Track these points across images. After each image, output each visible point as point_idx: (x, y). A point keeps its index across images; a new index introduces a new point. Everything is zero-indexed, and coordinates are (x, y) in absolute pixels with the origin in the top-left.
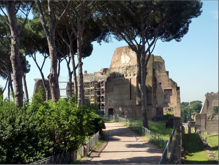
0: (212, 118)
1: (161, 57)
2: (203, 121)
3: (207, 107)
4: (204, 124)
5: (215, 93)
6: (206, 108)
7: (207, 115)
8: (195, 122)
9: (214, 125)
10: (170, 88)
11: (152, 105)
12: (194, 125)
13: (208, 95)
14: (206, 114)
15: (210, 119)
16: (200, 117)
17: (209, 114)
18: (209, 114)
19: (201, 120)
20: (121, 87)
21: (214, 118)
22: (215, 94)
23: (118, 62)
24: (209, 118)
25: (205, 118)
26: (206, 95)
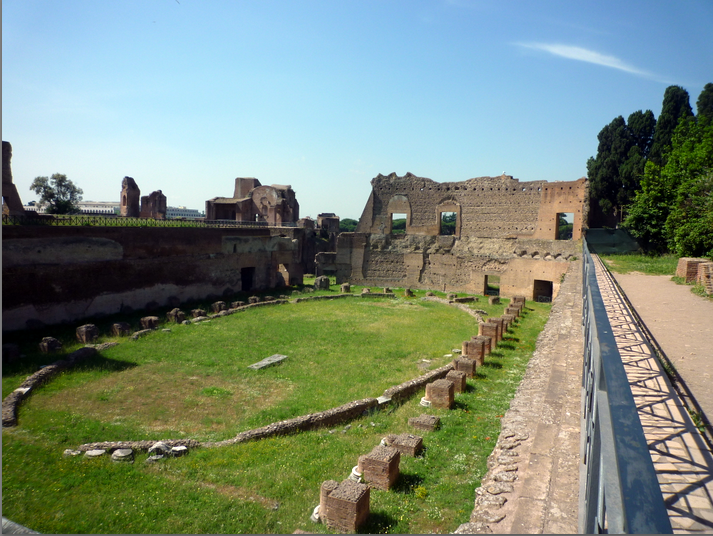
0: (384, 247)
2: (358, 255)
3: (374, 215)
4: (360, 262)
5: (399, 175)
6: (370, 216)
7: (372, 236)
9: (389, 266)
12: (333, 263)
14: (370, 234)
15: (379, 250)
16: (351, 243)
17: (377, 235)
18: (377, 235)
19: (354, 250)
21: (390, 247)
22: (399, 178)
24: (376, 247)
25: (366, 246)
26: (372, 182)
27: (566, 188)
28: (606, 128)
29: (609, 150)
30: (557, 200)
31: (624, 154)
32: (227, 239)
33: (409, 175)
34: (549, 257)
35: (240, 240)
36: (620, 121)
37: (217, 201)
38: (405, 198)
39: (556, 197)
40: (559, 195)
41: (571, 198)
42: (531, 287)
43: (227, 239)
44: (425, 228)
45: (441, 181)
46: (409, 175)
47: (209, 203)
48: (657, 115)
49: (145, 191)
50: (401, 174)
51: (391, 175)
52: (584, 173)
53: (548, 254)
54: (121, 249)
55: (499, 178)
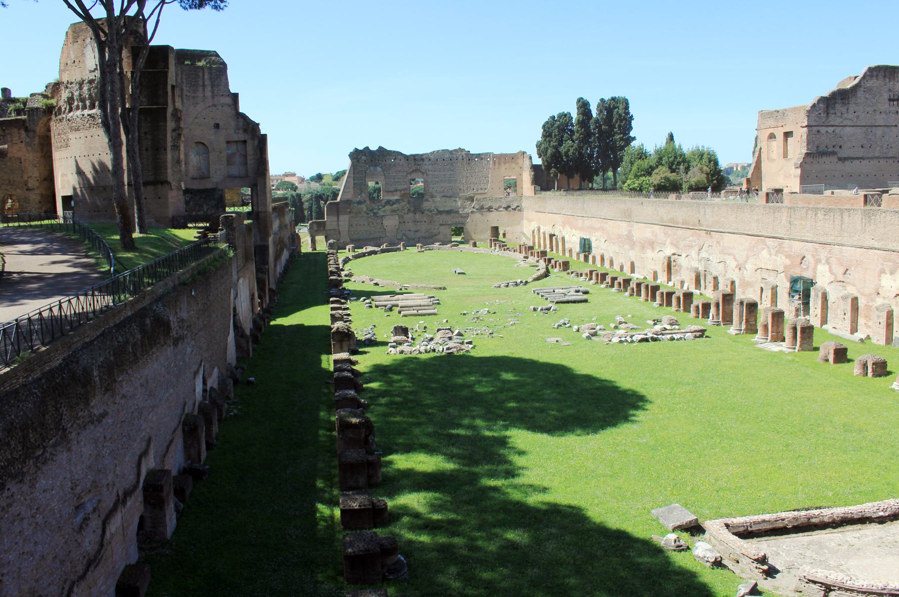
1: (217, 55)
8: (324, 223)
10: (241, 136)
11: (168, 183)
12: (324, 229)
20: (89, 137)
23: (75, 64)
27: (512, 158)
28: (547, 123)
29: (550, 136)
30: (503, 167)
31: (561, 142)
33: (381, 149)
34: (501, 209)
36: (553, 117)
38: (379, 169)
39: (502, 165)
40: (505, 163)
41: (514, 165)
44: (398, 192)
46: (380, 148)
48: (575, 115)
50: (374, 148)
51: (367, 148)
52: (533, 152)
53: (500, 207)
55: (455, 150)
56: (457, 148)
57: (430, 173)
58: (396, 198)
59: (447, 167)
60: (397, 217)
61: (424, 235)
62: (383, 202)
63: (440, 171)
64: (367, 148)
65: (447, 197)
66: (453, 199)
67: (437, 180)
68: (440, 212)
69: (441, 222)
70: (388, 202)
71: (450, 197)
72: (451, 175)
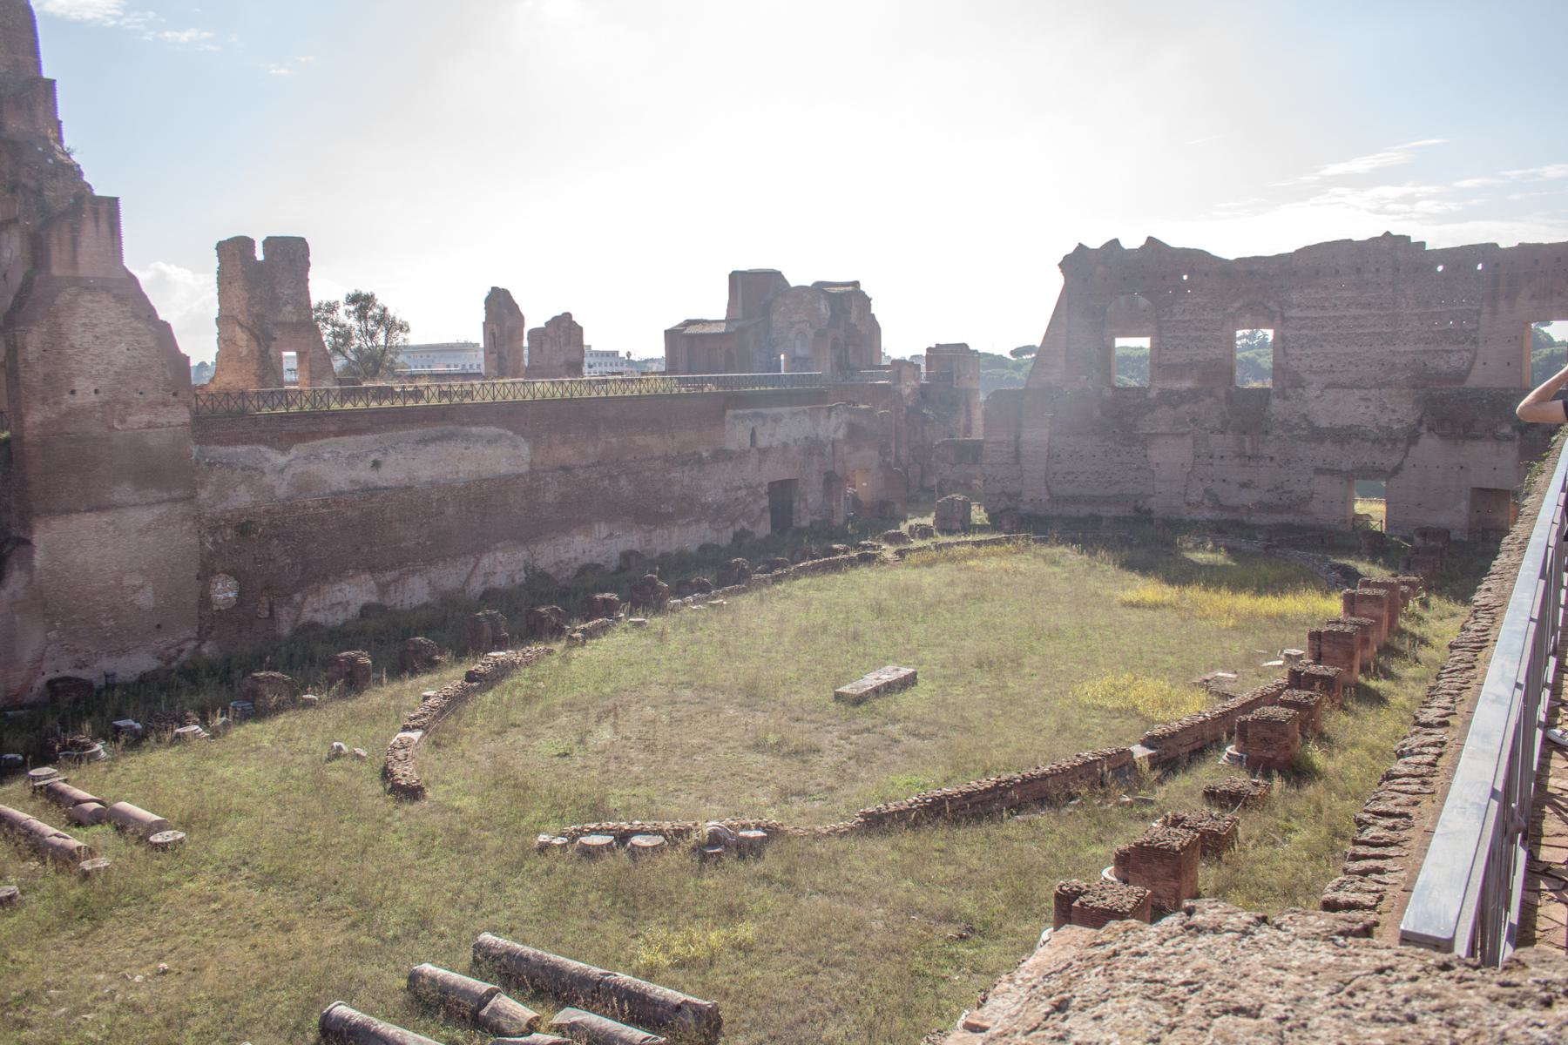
13: (1078, 264)
32: (736, 417)
33: (1150, 240)
35: (763, 416)
37: (691, 330)
42: (1464, 505)
43: (736, 417)
45: (1231, 256)
46: (1150, 240)
47: (671, 335)
49: (535, 317)
50: (1132, 241)
51: (1115, 242)
54: (525, 450)
56: (1380, 234)
57: (1294, 313)
58: (1188, 384)
59: (1345, 294)
60: (1189, 441)
61: (1267, 498)
62: (1153, 394)
63: (1323, 308)
64: (1115, 242)
65: (1343, 386)
66: (1358, 393)
67: (1313, 333)
68: (1318, 435)
69: (1319, 464)
70: (1169, 398)
71: (1350, 387)
72: (1355, 318)
